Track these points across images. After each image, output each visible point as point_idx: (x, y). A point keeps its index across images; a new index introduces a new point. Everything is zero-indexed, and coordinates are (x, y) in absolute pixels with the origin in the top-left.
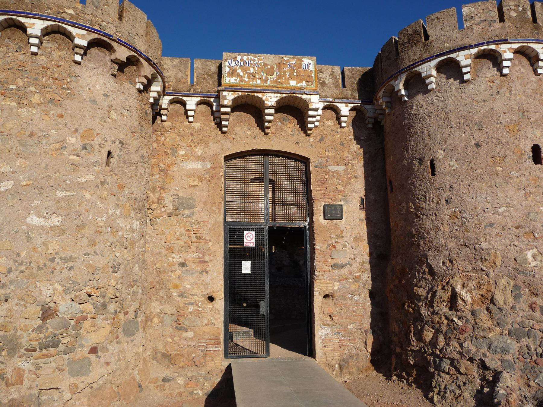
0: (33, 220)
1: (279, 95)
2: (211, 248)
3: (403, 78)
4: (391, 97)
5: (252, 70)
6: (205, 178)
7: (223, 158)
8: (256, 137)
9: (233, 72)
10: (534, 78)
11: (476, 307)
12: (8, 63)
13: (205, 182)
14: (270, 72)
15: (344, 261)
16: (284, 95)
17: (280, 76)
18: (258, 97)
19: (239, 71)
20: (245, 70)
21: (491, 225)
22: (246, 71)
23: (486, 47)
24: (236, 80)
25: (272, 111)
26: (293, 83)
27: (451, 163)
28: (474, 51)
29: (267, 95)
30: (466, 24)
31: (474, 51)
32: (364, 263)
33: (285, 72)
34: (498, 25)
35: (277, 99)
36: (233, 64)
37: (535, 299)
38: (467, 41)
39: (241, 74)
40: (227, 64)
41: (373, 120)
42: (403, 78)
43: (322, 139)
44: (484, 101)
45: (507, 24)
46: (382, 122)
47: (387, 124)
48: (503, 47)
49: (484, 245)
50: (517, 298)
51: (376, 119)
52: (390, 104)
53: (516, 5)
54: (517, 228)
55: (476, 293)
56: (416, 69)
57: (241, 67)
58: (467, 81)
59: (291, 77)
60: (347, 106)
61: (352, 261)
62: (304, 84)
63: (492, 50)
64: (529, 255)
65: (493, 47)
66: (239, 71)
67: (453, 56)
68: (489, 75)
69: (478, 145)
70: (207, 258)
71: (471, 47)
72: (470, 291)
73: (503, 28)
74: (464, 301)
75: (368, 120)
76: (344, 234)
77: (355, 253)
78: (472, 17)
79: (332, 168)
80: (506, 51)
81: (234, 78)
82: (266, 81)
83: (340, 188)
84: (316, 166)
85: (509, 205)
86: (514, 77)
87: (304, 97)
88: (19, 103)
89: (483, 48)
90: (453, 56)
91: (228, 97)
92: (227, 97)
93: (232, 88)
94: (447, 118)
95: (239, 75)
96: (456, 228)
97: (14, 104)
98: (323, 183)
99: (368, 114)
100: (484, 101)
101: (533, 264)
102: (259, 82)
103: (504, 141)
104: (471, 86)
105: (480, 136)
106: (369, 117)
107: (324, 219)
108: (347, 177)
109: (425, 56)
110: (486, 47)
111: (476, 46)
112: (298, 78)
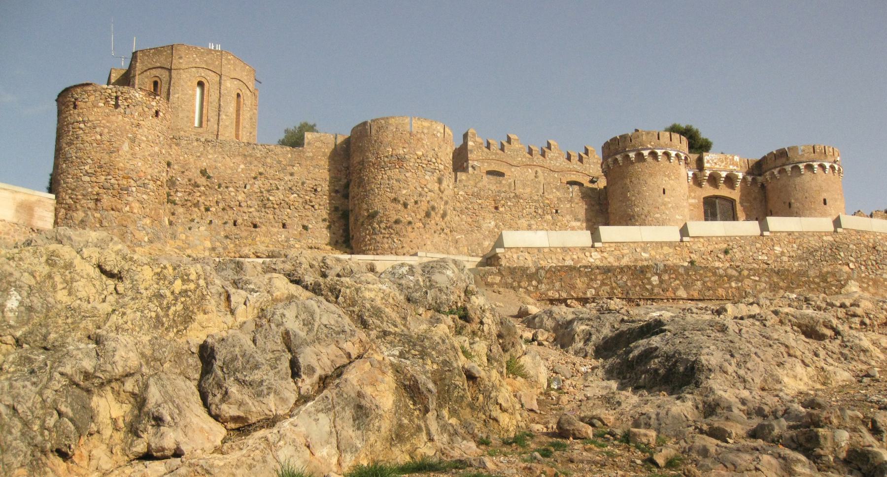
0: (677, 217)
3: (778, 169)
9: (708, 162)
26: (731, 167)
38: (802, 159)
47: (769, 187)
80: (816, 165)
91: (708, 173)
105: (807, 195)
112: (733, 164)
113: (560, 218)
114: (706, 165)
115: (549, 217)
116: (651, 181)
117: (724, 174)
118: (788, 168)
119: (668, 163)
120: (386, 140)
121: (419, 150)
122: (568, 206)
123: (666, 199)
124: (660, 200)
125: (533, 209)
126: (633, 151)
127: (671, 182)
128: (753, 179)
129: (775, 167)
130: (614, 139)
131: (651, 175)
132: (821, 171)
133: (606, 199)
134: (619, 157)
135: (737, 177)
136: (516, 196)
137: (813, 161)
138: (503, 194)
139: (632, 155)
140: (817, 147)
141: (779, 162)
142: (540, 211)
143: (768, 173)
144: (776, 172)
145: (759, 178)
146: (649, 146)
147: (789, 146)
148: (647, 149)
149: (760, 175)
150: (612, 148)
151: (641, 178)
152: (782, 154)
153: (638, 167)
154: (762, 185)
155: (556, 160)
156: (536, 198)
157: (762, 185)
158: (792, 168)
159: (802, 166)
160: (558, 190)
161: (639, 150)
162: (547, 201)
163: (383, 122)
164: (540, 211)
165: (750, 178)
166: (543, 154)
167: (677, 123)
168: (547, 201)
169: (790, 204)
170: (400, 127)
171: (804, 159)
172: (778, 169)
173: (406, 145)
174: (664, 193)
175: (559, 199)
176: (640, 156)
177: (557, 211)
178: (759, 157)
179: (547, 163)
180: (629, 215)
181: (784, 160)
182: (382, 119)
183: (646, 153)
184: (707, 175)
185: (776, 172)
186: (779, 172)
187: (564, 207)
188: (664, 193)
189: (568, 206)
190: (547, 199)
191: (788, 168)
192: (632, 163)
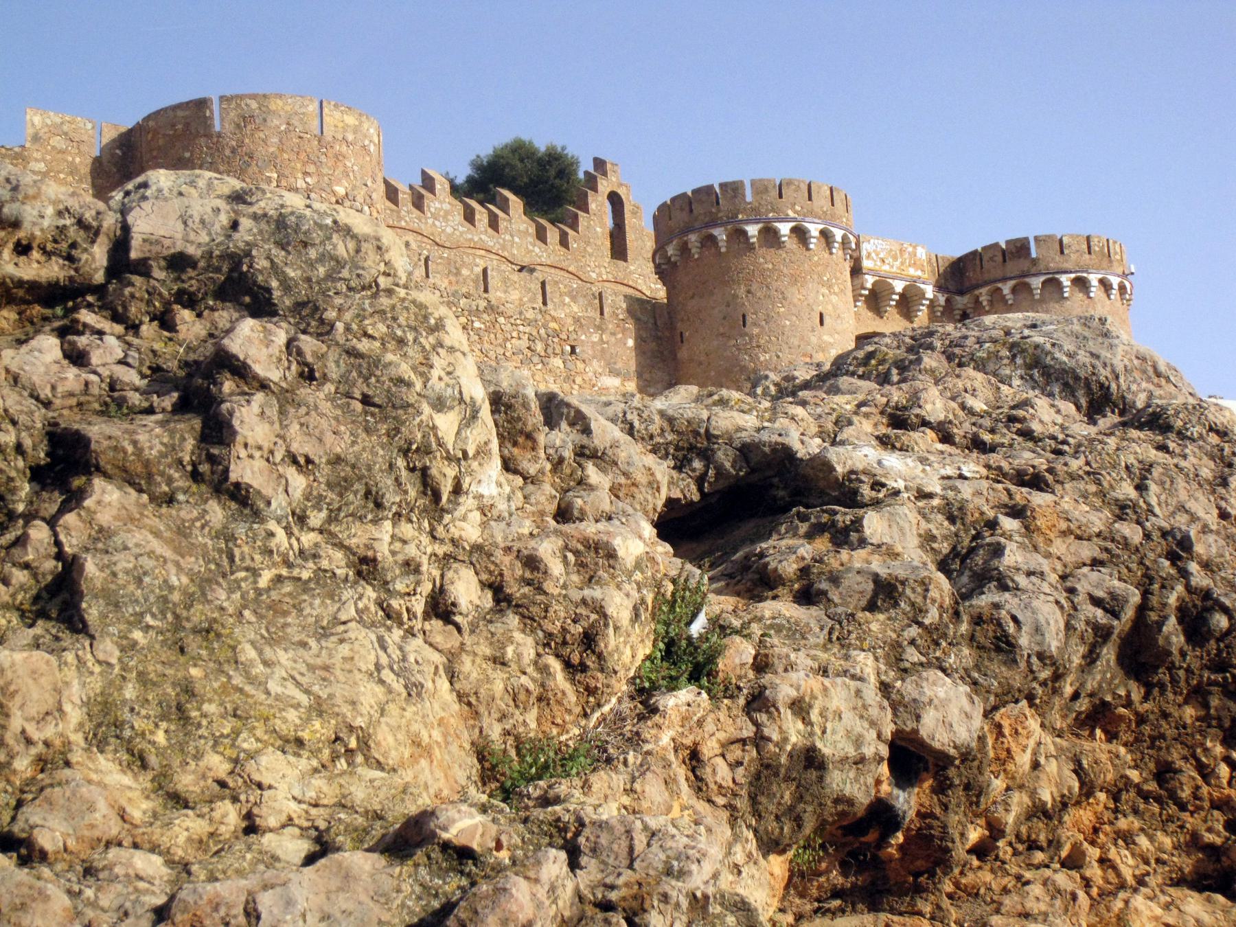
3: (1012, 283)
5: (882, 256)
10: (1108, 302)
14: (895, 259)
17: (902, 263)
25: (897, 297)
26: (912, 272)
28: (1073, 276)
30: (1066, 251)
31: (1073, 276)
34: (1087, 256)
42: (1012, 283)
45: (1093, 256)
52: (991, 302)
56: (1027, 280)
58: (1066, 298)
62: (919, 273)
75: (957, 312)
87: (922, 286)
93: (872, 272)
99: (959, 306)
109: (1033, 271)
113: (580, 365)
114: (866, 264)
115: (557, 362)
116: (794, 295)
117: (899, 286)
118: (1036, 282)
119: (826, 255)
120: (261, 152)
121: (339, 183)
122: (595, 338)
123: (826, 338)
124: (814, 340)
125: (524, 343)
126: (757, 222)
127: (834, 299)
128: (947, 301)
129: (1005, 279)
130: (705, 192)
131: (794, 280)
132: (1103, 295)
133: (671, 326)
134: (721, 234)
135: (922, 295)
136: (490, 308)
138: (463, 301)
139: (753, 230)
140: (1094, 242)
141: (1013, 267)
142: (539, 347)
143: (984, 290)
144: (1006, 288)
145: (958, 298)
147: (1041, 232)
149: (961, 293)
150: (698, 209)
151: (775, 285)
152: (1019, 248)
153: (765, 258)
155: (445, 218)
156: (530, 315)
158: (1044, 283)
159: (1065, 280)
160: (574, 299)
161: (768, 222)
162: (553, 325)
163: (254, 105)
164: (539, 347)
165: (942, 300)
166: (418, 202)
167: (525, 137)
168: (553, 325)
170: (295, 122)
172: (1012, 283)
173: (311, 168)
174: (822, 323)
175: (577, 320)
176: (770, 235)
177: (573, 348)
178: (958, 253)
179: (428, 224)
180: (743, 369)
181: (1024, 265)
182: (254, 97)
183: (784, 228)
184: (869, 285)
185: (1006, 288)
186: (1014, 290)
187: (589, 339)
188: (822, 323)
189: (595, 338)
190: (554, 319)
191: (1036, 282)
192: (751, 247)
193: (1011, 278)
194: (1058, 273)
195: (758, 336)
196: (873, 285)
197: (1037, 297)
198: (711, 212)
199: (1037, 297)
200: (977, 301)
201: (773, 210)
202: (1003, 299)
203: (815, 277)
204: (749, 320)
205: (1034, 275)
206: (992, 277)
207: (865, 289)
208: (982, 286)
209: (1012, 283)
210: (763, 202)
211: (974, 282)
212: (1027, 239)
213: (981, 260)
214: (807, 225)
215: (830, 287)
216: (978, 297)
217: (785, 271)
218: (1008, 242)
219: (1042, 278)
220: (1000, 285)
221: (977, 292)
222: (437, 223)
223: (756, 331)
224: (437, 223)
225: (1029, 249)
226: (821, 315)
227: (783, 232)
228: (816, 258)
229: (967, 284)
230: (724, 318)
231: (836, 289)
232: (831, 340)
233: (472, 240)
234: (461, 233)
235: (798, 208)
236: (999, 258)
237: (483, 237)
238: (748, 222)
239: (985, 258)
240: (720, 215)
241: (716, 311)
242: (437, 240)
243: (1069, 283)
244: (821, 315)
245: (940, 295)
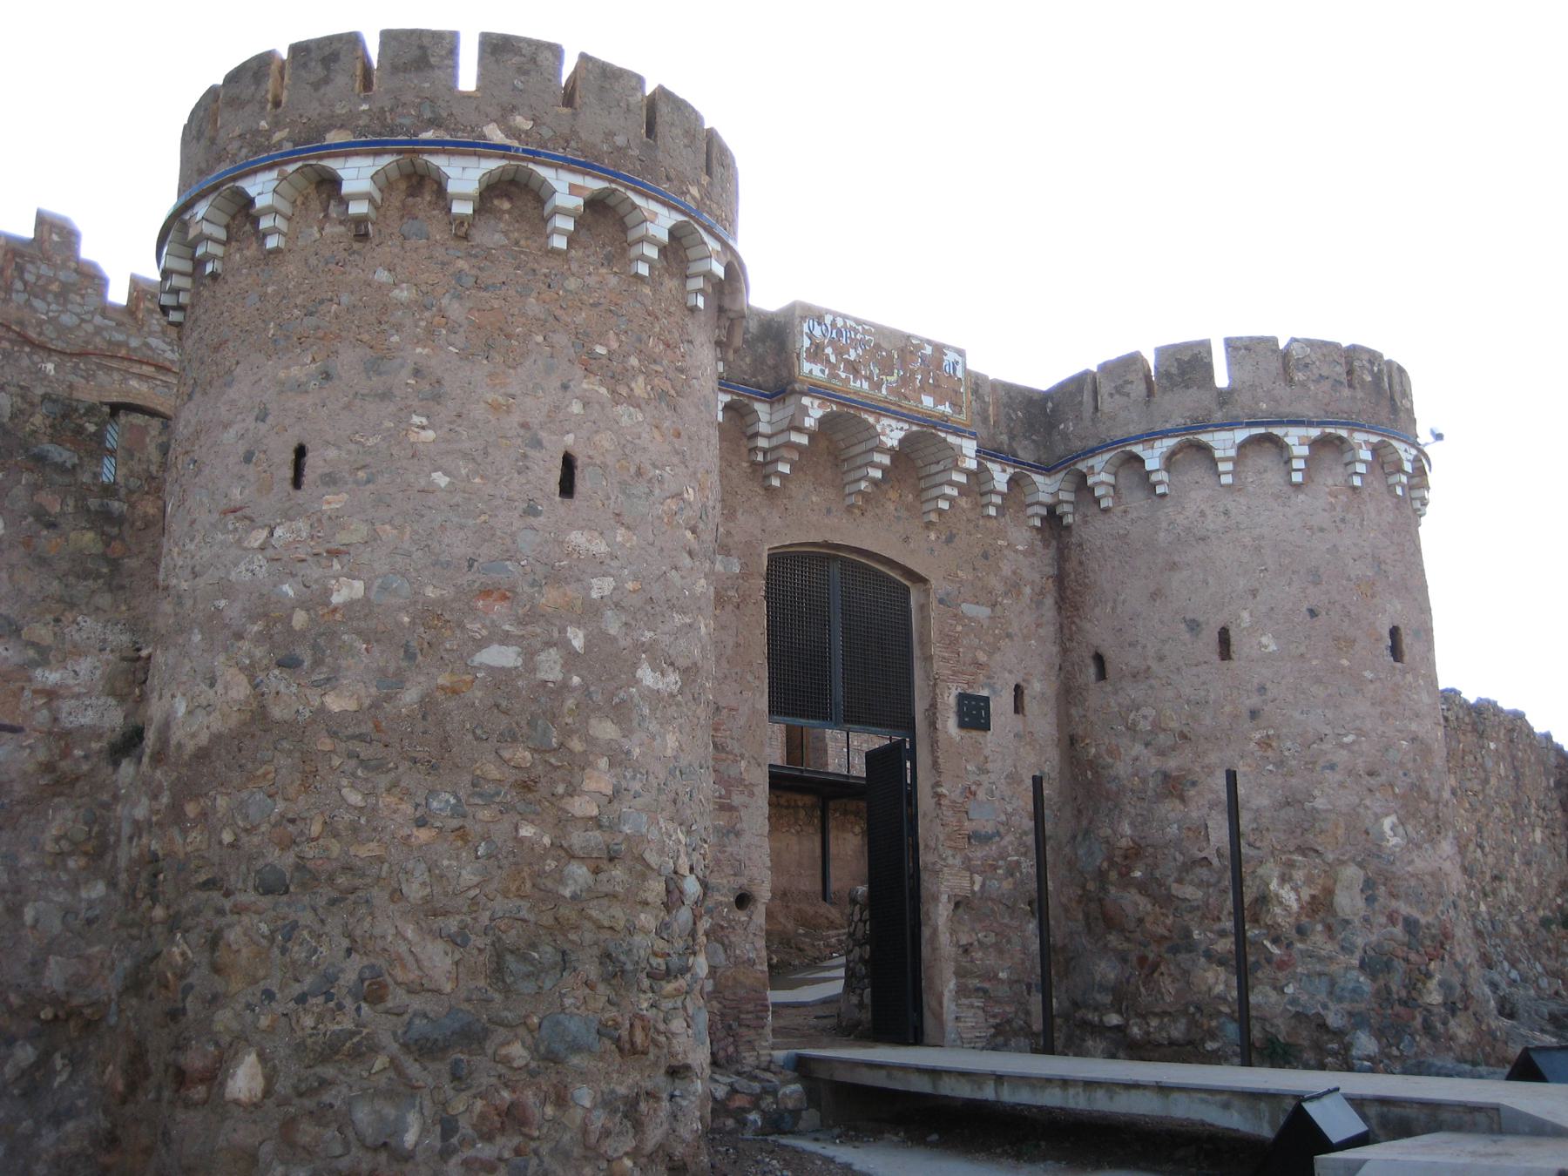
1: (906, 426)
2: (745, 776)
4: (1115, 475)
5: (852, 355)
6: (730, 598)
7: (765, 555)
8: (829, 511)
9: (816, 353)
11: (1304, 920)
12: (589, 290)
13: (729, 608)
15: (989, 828)
16: (915, 428)
17: (904, 381)
18: (866, 421)
19: (829, 350)
20: (839, 352)
21: (1332, 767)
22: (841, 354)
23: (1332, 430)
24: (823, 371)
26: (928, 401)
27: (1264, 640)
28: (1314, 432)
29: (885, 421)
31: (1314, 432)
32: (1025, 833)
33: (913, 373)
34: (1346, 392)
35: (901, 434)
36: (817, 332)
37: (1394, 904)
39: (833, 359)
40: (806, 329)
41: (1044, 512)
43: (950, 539)
44: (1322, 530)
46: (1069, 519)
47: (1094, 533)
48: (1359, 437)
49: (1320, 803)
50: (1370, 900)
51: (1051, 509)
53: (1371, 363)
54: (1371, 774)
55: (1306, 894)
57: (832, 342)
59: (922, 389)
60: (1004, 471)
61: (1002, 829)
62: (946, 408)
63: (1340, 438)
64: (1387, 823)
65: (1343, 433)
66: (829, 350)
67: (1277, 431)
68: (1330, 482)
69: (1312, 613)
70: (737, 799)
71: (1310, 424)
72: (1295, 889)
73: (1354, 398)
74: (1286, 909)
76: (990, 766)
77: (1010, 809)
78: (1306, 366)
79: (968, 608)
81: (819, 367)
82: (878, 386)
83: (982, 657)
84: (941, 601)
85: (1360, 732)
86: (1365, 495)
88: (613, 392)
89: (1328, 430)
90: (1277, 431)
92: (811, 412)
94: (1258, 549)
95: (828, 361)
96: (1270, 767)
97: (603, 390)
98: (952, 642)
100: (1322, 530)
101: (1394, 841)
102: (866, 385)
103: (1353, 611)
104: (1301, 497)
106: (1038, 503)
107: (962, 725)
108: (995, 636)
110: (1332, 430)
111: (1319, 424)
112: (935, 390)
123: (577, 538)
127: (627, 416)
128: (1013, 482)
129: (1149, 437)
137: (1354, 426)
143: (1098, 462)
146: (495, 134)
148: (477, 147)
154: (1052, 518)
157: (1052, 518)
158: (1242, 446)
161: (414, 147)
169: (1224, 639)
171: (1306, 409)
172: (1170, 443)
174: (567, 487)
186: (1170, 460)
188: (567, 487)
193: (1165, 434)
194: (1280, 423)
195: (334, 518)
196: (821, 421)
197: (1226, 479)
198: (257, 132)
199: (1226, 479)
200: (1081, 485)
201: (435, 123)
202: (1146, 482)
203: (561, 339)
204: (314, 465)
205: (1221, 427)
206: (1119, 434)
207: (800, 430)
208: (1092, 452)
209: (1170, 443)
210: (408, 97)
211: (1077, 445)
212: (1205, 346)
213: (1095, 393)
214: (543, 172)
215: (616, 378)
216: (1084, 477)
217: (455, 310)
218: (1161, 352)
219: (1241, 435)
220: (1137, 449)
221: (1082, 466)
222: (37, 303)
223: (334, 502)
224: (37, 303)
225: (1208, 368)
226: (568, 463)
227: (452, 187)
228: (572, 284)
229: (1060, 449)
230: (248, 458)
231: (639, 387)
232: (601, 547)
233: (119, 344)
234: (99, 330)
235: (522, 122)
236: (1139, 389)
237: (154, 342)
238: (346, 151)
239: (1105, 389)
240: (277, 136)
241: (229, 436)
242: (32, 334)
243: (1305, 451)
244: (568, 463)
245: (995, 468)
